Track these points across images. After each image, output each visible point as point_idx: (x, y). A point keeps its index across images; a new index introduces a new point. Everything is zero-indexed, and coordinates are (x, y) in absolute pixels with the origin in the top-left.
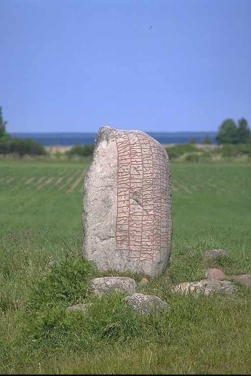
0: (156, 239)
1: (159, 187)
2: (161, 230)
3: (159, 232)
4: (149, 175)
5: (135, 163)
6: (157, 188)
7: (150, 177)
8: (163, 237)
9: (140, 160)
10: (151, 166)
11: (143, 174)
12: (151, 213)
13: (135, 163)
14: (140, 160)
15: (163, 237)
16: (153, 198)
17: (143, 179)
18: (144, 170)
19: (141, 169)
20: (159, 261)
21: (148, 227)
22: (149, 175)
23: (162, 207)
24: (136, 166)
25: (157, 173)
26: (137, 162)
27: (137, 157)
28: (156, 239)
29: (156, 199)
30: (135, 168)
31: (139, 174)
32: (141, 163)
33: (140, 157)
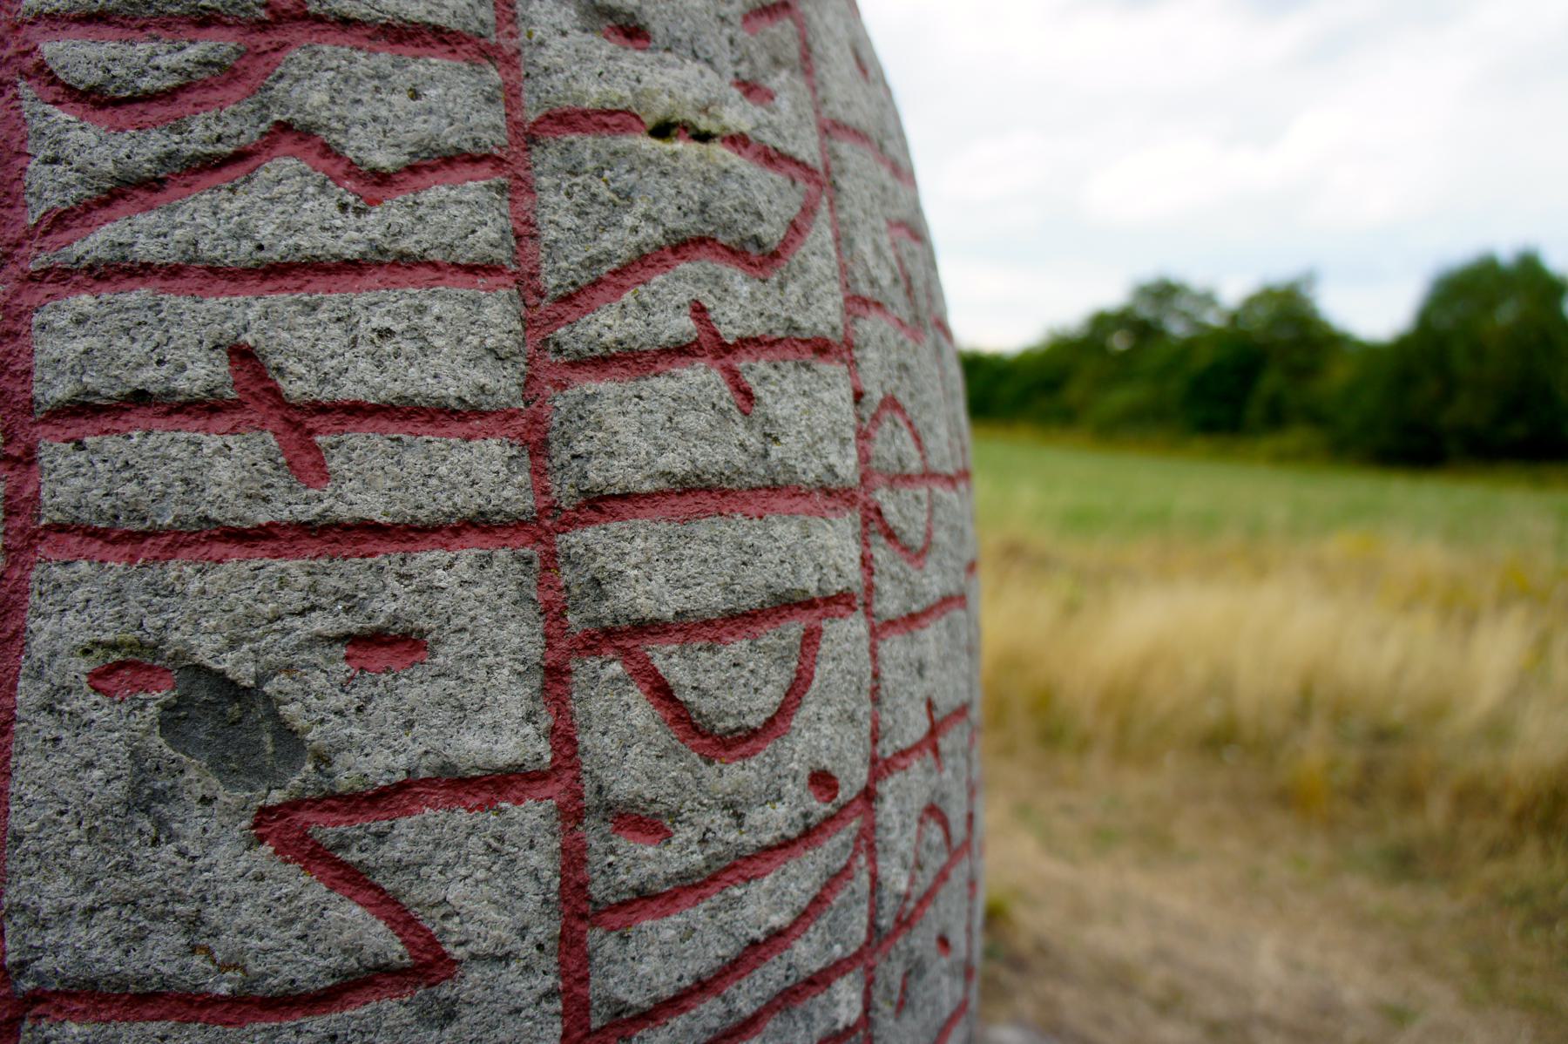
4: (762, 905)
5: (231, 470)
9: (457, 344)
11: (581, 910)
13: (231, 470)
14: (457, 344)
18: (626, 742)
19: (511, 739)
22: (762, 905)
24: (213, 612)
26: (306, 425)
27: (286, 208)
30: (221, 713)
31: (428, 966)
32: (483, 471)
33: (461, 214)
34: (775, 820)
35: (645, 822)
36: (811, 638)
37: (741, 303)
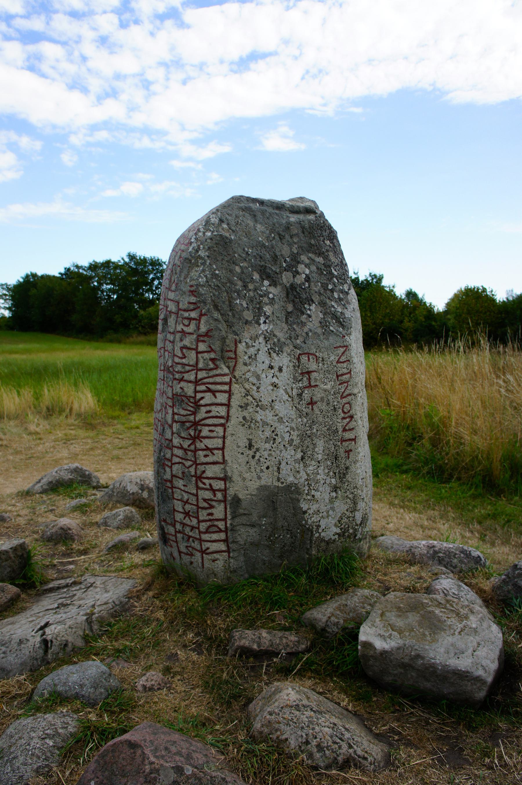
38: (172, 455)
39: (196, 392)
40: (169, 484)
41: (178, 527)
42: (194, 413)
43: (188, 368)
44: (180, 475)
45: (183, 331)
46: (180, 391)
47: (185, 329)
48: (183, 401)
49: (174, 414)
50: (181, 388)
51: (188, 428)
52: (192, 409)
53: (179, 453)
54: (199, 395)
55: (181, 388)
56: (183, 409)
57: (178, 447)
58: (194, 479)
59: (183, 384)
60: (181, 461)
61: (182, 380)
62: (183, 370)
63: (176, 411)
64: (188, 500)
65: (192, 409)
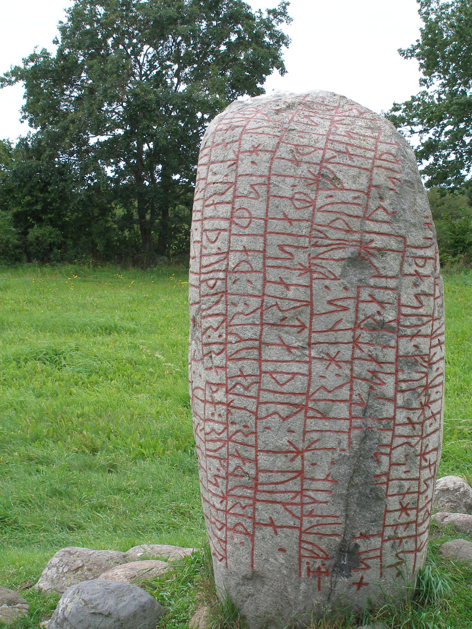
0: (238, 492)
1: (254, 303)
2: (256, 461)
3: (249, 468)
6: (240, 308)
7: (216, 267)
8: (265, 488)
10: (224, 224)
12: (220, 396)
15: (265, 488)
16: (225, 343)
17: (200, 273)
20: (245, 570)
21: (211, 446)
23: (266, 379)
25: (245, 251)
28: (238, 492)
29: (235, 347)
34: (214, 251)
35: (206, 248)
36: (219, 233)
37: (217, 199)
38: (394, 436)
39: (431, 347)
40: (384, 479)
41: (389, 532)
42: (427, 375)
43: (425, 319)
44: (403, 460)
45: (417, 273)
46: (414, 349)
47: (420, 270)
48: (417, 361)
49: (397, 382)
50: (415, 346)
51: (419, 395)
52: (425, 370)
53: (406, 430)
54: (433, 351)
55: (415, 346)
56: (417, 372)
57: (404, 424)
58: (419, 458)
59: (418, 340)
60: (405, 440)
61: (417, 335)
62: (419, 323)
63: (401, 376)
64: (409, 489)
65: (425, 370)
